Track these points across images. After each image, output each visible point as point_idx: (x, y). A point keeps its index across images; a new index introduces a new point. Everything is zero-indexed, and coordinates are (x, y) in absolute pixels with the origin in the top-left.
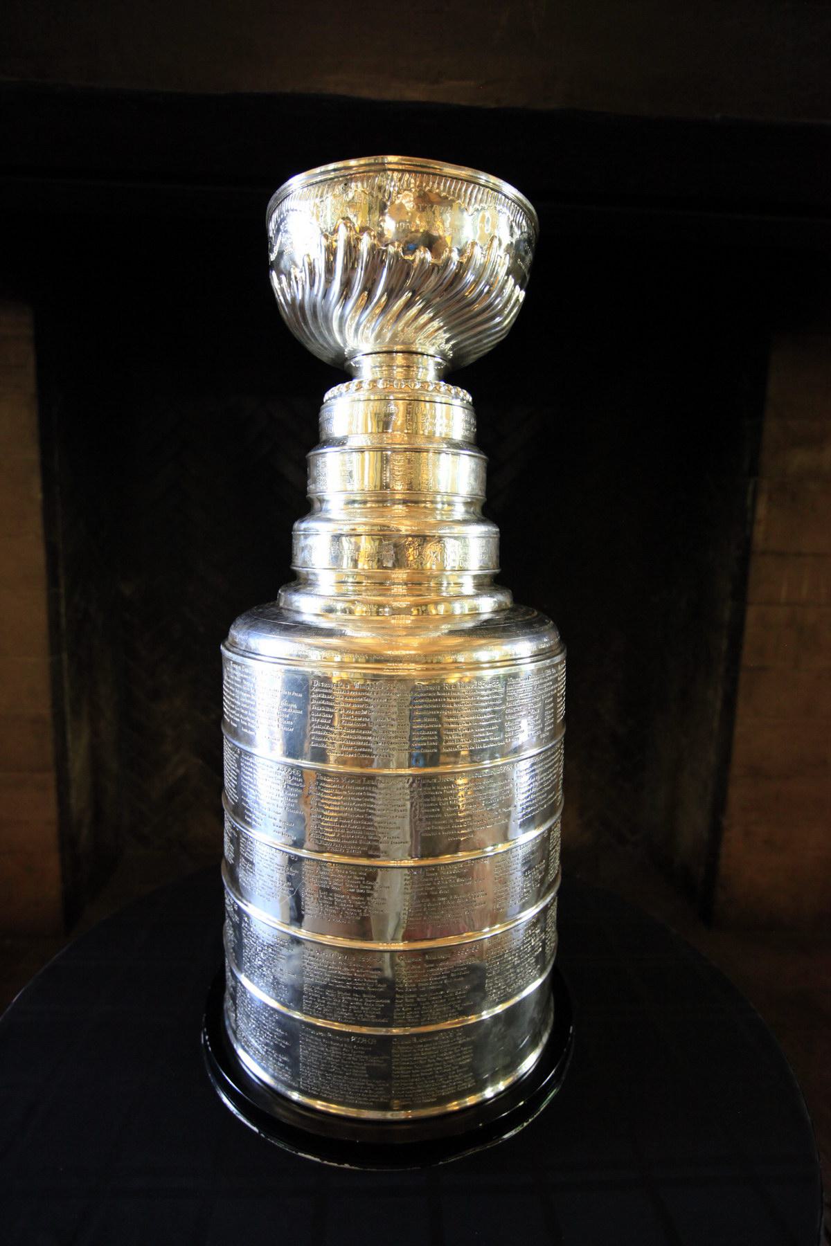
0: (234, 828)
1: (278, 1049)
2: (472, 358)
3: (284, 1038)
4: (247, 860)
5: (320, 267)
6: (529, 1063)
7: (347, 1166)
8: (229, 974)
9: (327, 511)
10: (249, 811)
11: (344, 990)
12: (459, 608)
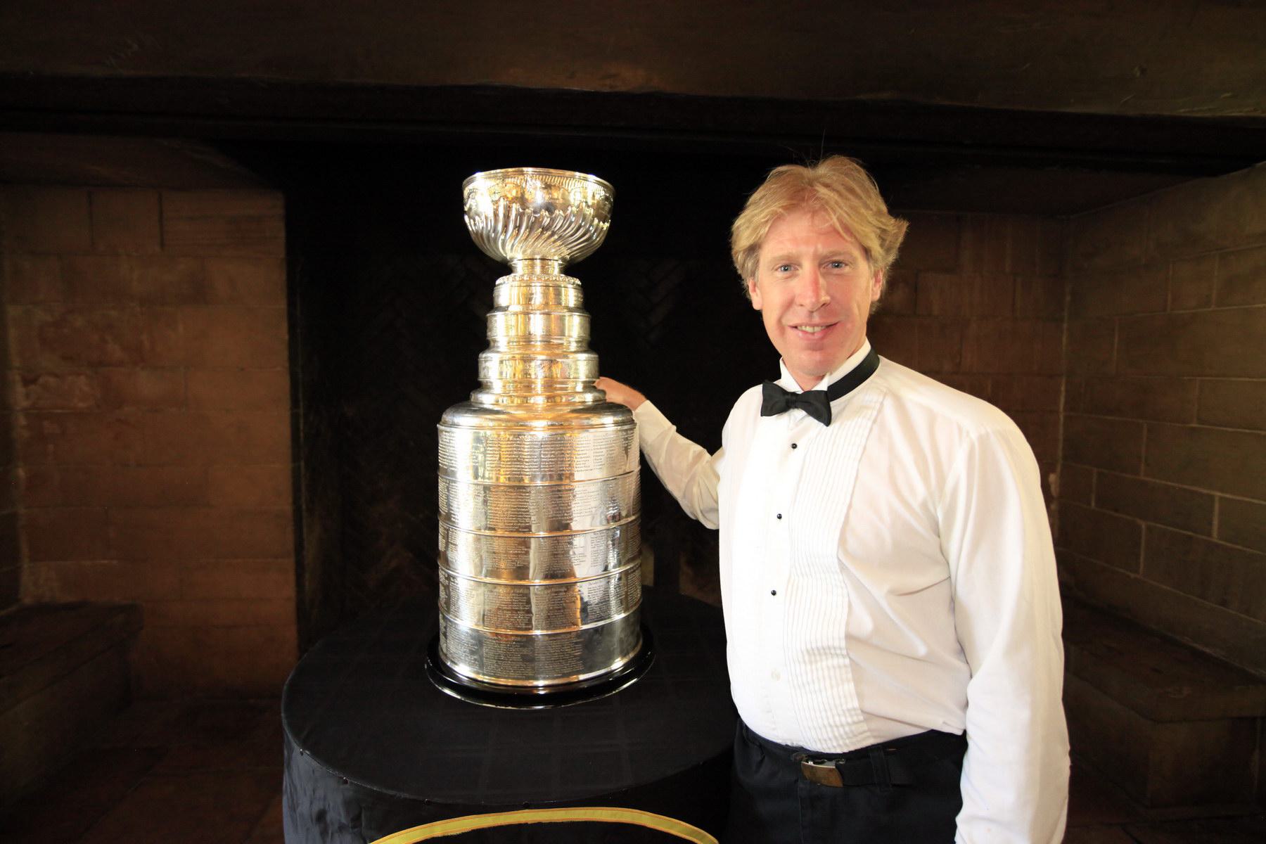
0: (445, 529)
1: (472, 653)
2: (581, 259)
3: (476, 645)
4: (452, 543)
5: (491, 216)
6: (618, 664)
7: (510, 708)
8: (441, 621)
9: (498, 347)
10: (454, 515)
11: (508, 610)
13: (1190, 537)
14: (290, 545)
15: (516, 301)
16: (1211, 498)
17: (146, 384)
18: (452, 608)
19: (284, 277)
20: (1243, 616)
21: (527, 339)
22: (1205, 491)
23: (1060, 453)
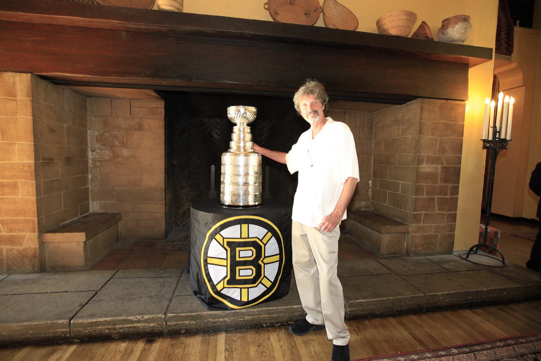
12: (248, 150)
13: (396, 193)
14: (164, 198)
15: (238, 130)
16: (399, 183)
17: (125, 152)
18: (225, 191)
19: (164, 124)
20: (404, 211)
21: (240, 137)
22: (398, 181)
23: (372, 175)
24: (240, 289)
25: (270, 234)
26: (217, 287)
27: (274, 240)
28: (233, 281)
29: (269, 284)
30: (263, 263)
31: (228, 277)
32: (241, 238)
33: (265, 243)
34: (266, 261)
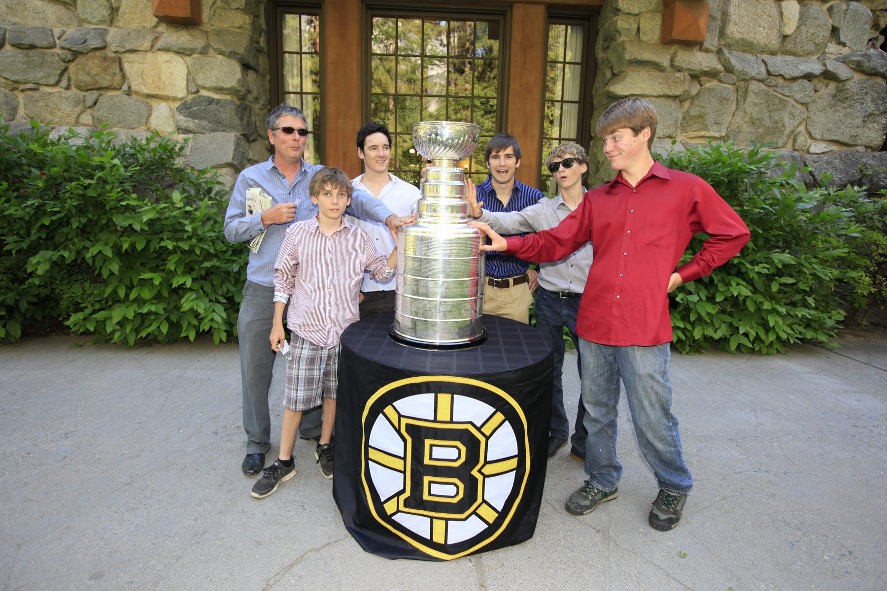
24: (429, 519)
25: (500, 417)
26: (385, 505)
27: (507, 427)
28: (416, 502)
29: (491, 517)
30: (482, 474)
31: (408, 494)
32: (435, 420)
33: (488, 434)
34: (488, 470)
